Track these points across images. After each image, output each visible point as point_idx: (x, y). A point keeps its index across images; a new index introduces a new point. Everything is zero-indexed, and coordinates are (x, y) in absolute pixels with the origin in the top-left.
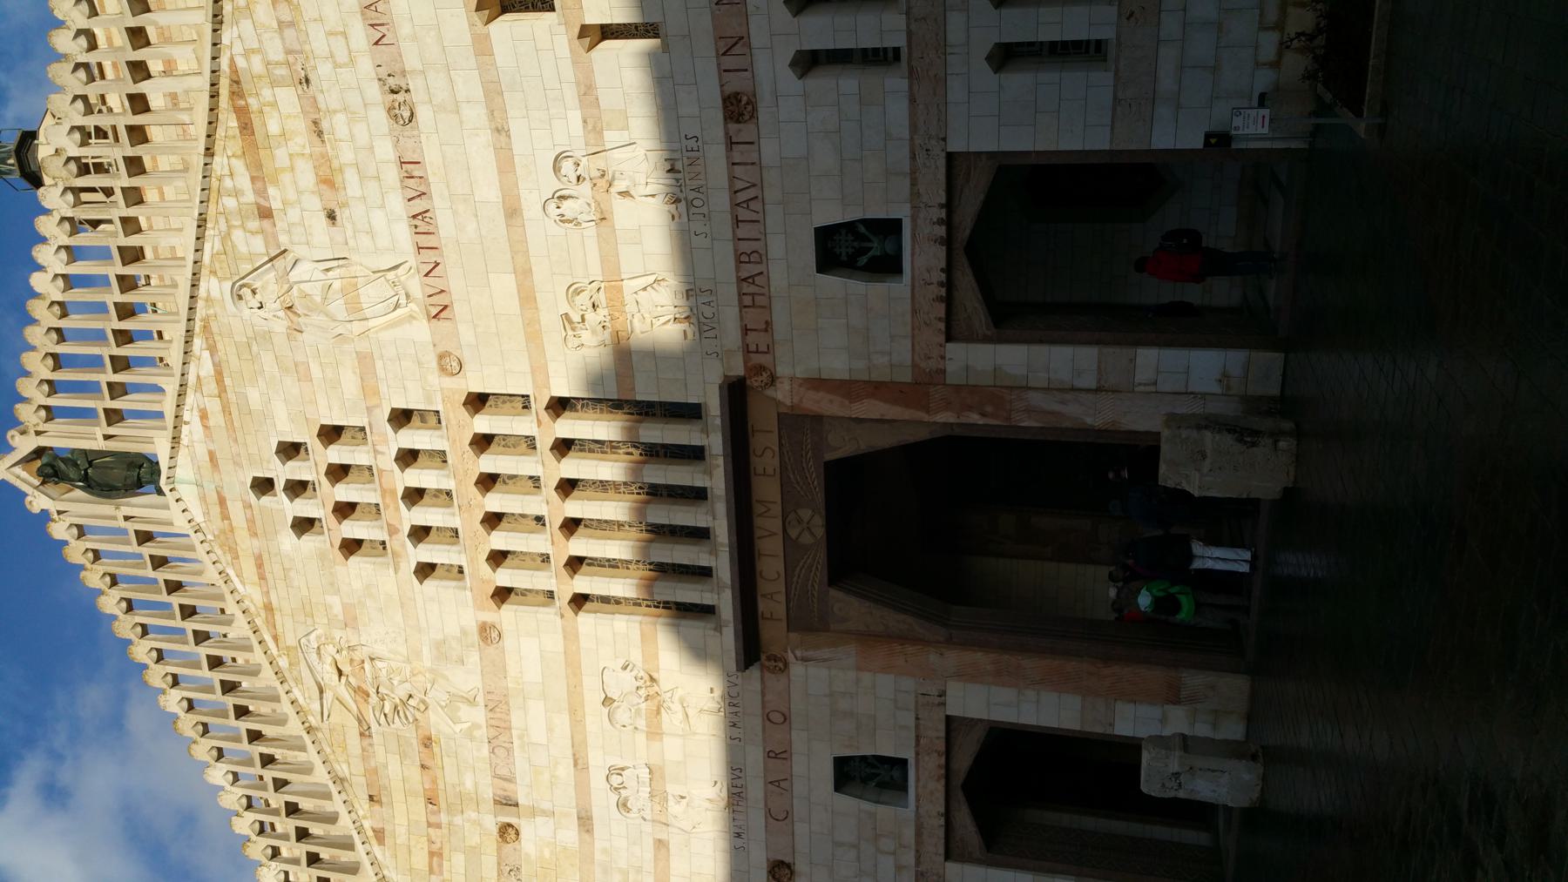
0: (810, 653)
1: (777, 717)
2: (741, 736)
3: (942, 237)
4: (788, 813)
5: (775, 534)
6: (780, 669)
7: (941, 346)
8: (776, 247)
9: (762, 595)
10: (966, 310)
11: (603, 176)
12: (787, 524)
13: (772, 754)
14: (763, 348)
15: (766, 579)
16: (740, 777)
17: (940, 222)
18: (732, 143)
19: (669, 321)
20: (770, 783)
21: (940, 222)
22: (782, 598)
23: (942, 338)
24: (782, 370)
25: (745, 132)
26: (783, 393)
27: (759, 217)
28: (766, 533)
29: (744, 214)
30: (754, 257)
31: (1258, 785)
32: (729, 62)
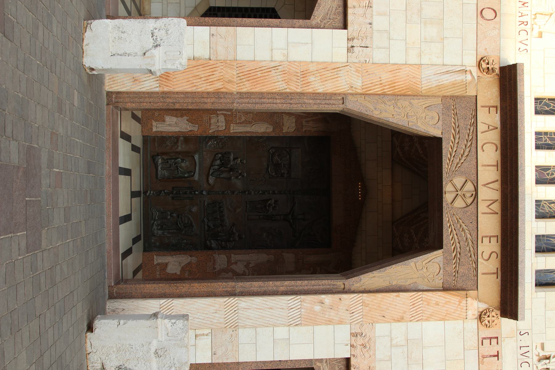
0: (460, 78)
1: (488, 14)
5: (484, 185)
7: (354, 356)
9: (497, 128)
12: (474, 193)
14: (486, 342)
15: (492, 143)
22: (481, 127)
23: (353, 362)
24: (473, 324)
28: (490, 185)
31: (87, 45)
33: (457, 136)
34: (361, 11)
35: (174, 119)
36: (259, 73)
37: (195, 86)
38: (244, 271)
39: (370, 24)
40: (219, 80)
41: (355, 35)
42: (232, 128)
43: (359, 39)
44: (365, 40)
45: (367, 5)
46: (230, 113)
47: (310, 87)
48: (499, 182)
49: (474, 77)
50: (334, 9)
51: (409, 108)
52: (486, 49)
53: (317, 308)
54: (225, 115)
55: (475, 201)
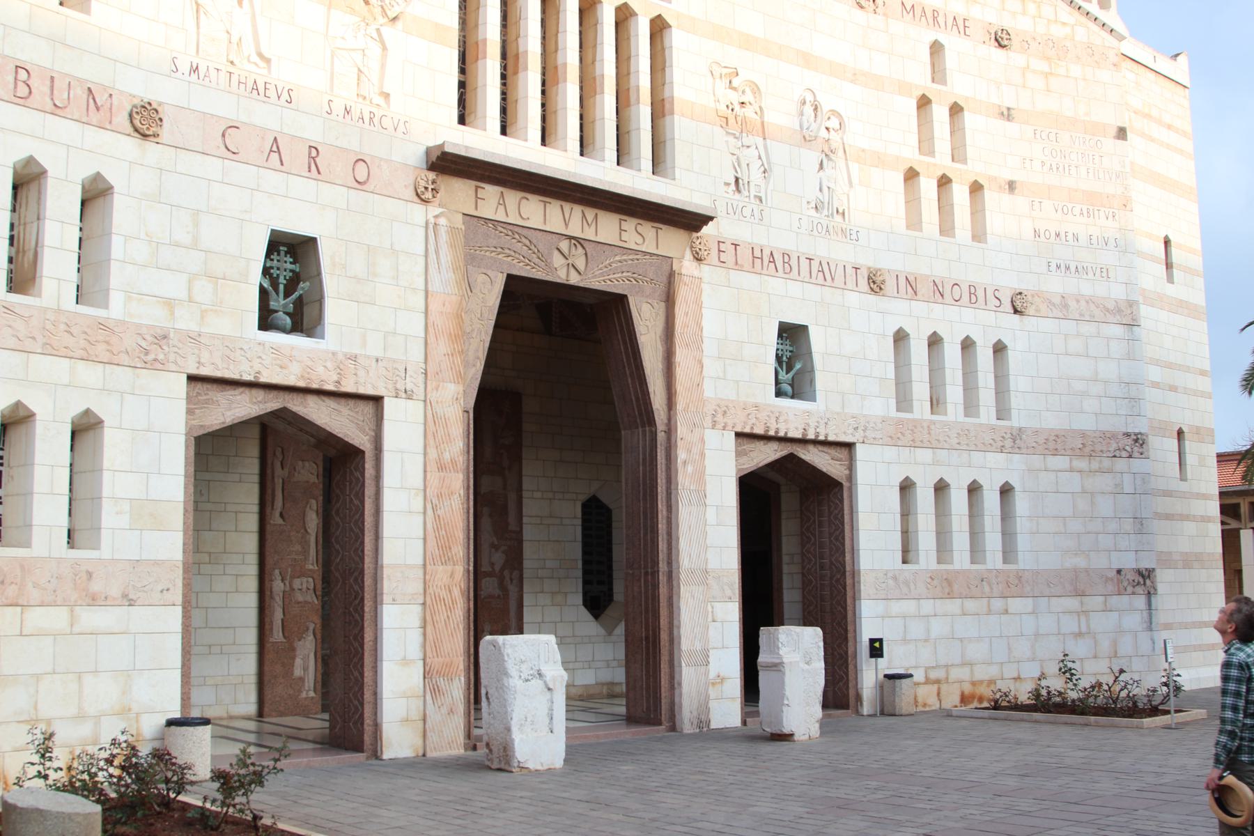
1: (361, 172)
2: (333, 116)
3: (807, 435)
4: (234, 153)
5: (566, 225)
6: (423, 194)
7: (733, 427)
8: (795, 288)
9: (502, 193)
10: (751, 451)
11: (832, 151)
12: (573, 241)
13: (314, 153)
14: (723, 256)
16: (279, 98)
17: (817, 434)
18: (856, 268)
19: (737, 172)
20: (275, 138)
21: (817, 434)
22: (500, 216)
23: (739, 429)
24: (705, 271)
25: (863, 282)
26: (687, 266)
27: (813, 280)
29: (815, 265)
30: (788, 269)
31: (542, 765)
32: (902, 281)
33: (507, 251)
34: (361, 373)
35: (298, 662)
36: (444, 532)
37: (458, 625)
38: (503, 552)
39: (377, 361)
40: (450, 591)
41: (390, 386)
42: (311, 567)
43: (397, 381)
44: (397, 373)
45: (353, 363)
46: (290, 570)
47: (457, 459)
48: (564, 204)
49: (441, 213)
50: (351, 414)
51: (473, 316)
52: (405, 186)
53: (690, 469)
54: (293, 577)
55: (582, 242)
